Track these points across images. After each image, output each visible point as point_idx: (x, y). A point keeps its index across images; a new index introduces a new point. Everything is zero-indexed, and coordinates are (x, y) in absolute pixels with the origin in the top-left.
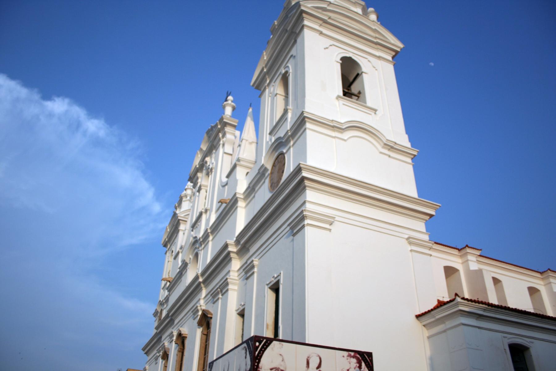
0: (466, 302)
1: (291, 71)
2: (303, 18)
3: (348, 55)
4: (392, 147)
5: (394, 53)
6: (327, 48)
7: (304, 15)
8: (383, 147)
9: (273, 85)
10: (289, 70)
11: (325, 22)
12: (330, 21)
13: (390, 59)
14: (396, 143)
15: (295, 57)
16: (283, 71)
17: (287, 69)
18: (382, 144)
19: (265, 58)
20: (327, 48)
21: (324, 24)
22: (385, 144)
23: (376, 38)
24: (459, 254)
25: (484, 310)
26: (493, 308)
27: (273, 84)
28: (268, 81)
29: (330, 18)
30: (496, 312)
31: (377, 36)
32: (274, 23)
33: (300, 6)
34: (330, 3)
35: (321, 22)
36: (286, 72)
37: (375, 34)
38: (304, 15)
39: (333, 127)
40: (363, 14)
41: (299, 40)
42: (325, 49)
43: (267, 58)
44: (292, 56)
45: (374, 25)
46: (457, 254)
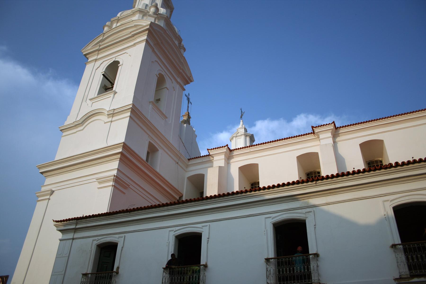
0: (60, 223)
3: (112, 61)
4: (113, 114)
7: (87, 56)
8: (108, 118)
11: (99, 50)
12: (101, 47)
14: (114, 110)
18: (107, 115)
21: (100, 52)
22: (108, 115)
24: (316, 137)
25: (65, 225)
26: (71, 221)
30: (86, 222)
35: (97, 52)
39: (76, 126)
46: (314, 137)
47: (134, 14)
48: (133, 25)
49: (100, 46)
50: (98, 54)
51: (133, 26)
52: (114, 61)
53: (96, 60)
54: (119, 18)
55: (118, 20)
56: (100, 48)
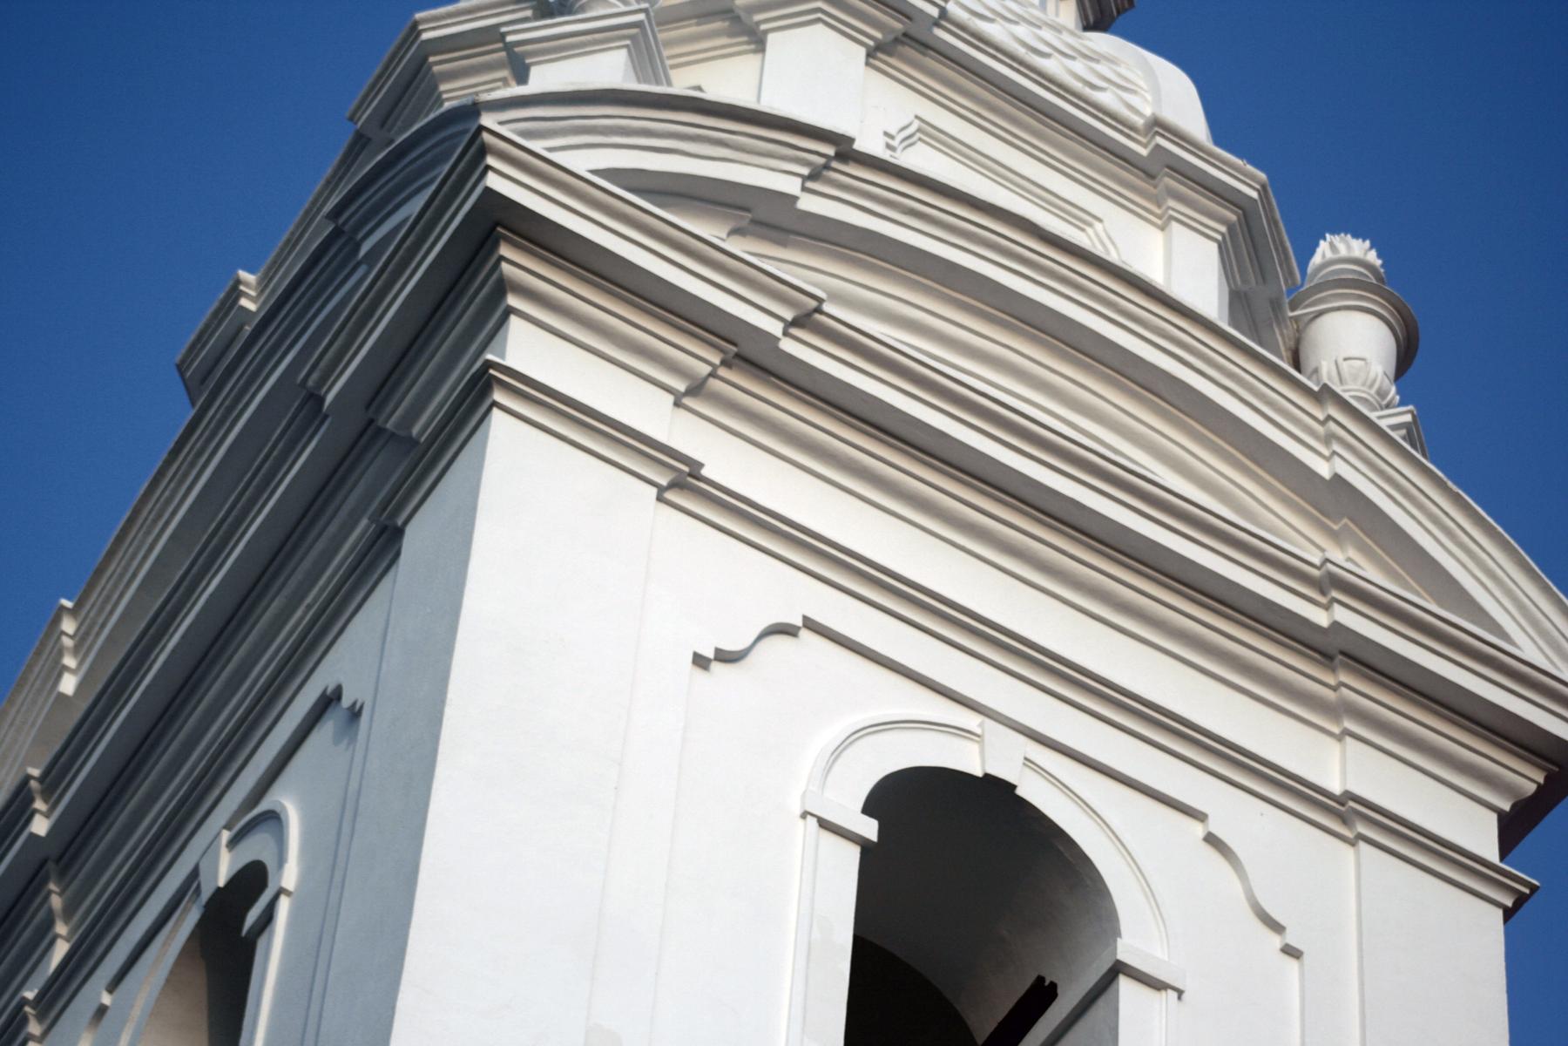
1: (290, 876)
2: (503, 287)
3: (969, 760)
5: (1527, 779)
6: (724, 657)
7: (514, 261)
9: (102, 1011)
10: (281, 860)
12: (801, 350)
13: (1482, 838)
15: (355, 714)
16: (224, 868)
17: (257, 848)
19: (68, 685)
20: (724, 657)
21: (739, 385)
23: (1330, 584)
27: (106, 999)
28: (61, 950)
29: (806, 320)
31: (1349, 559)
32: (235, 292)
33: (476, 154)
34: (845, 150)
35: (700, 357)
36: (252, 879)
37: (1335, 536)
38: (514, 261)
40: (1238, 301)
41: (418, 537)
42: (700, 661)
43: (80, 687)
44: (329, 701)
45: (1329, 439)
47: (1150, 176)
48: (1324, 469)
49: (795, 323)
50: (697, 389)
51: (1321, 478)
52: (997, 790)
53: (673, 485)
54: (939, 32)
55: (907, 38)
56: (787, 345)
